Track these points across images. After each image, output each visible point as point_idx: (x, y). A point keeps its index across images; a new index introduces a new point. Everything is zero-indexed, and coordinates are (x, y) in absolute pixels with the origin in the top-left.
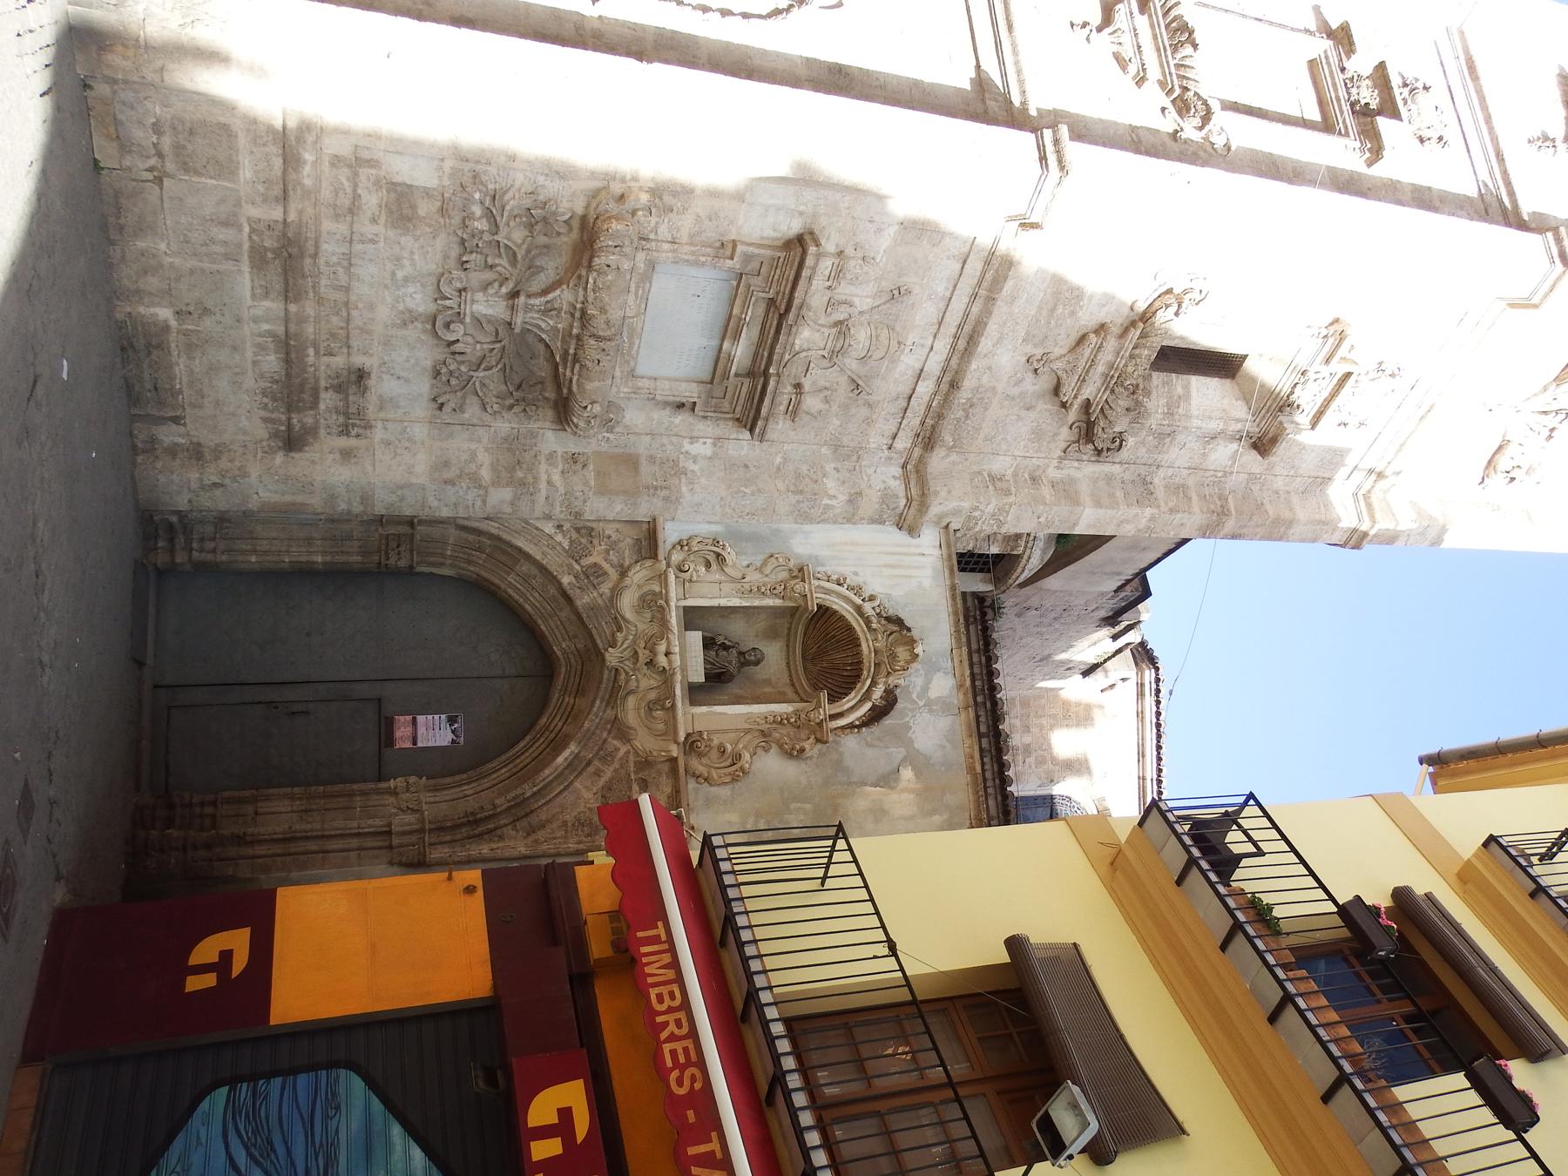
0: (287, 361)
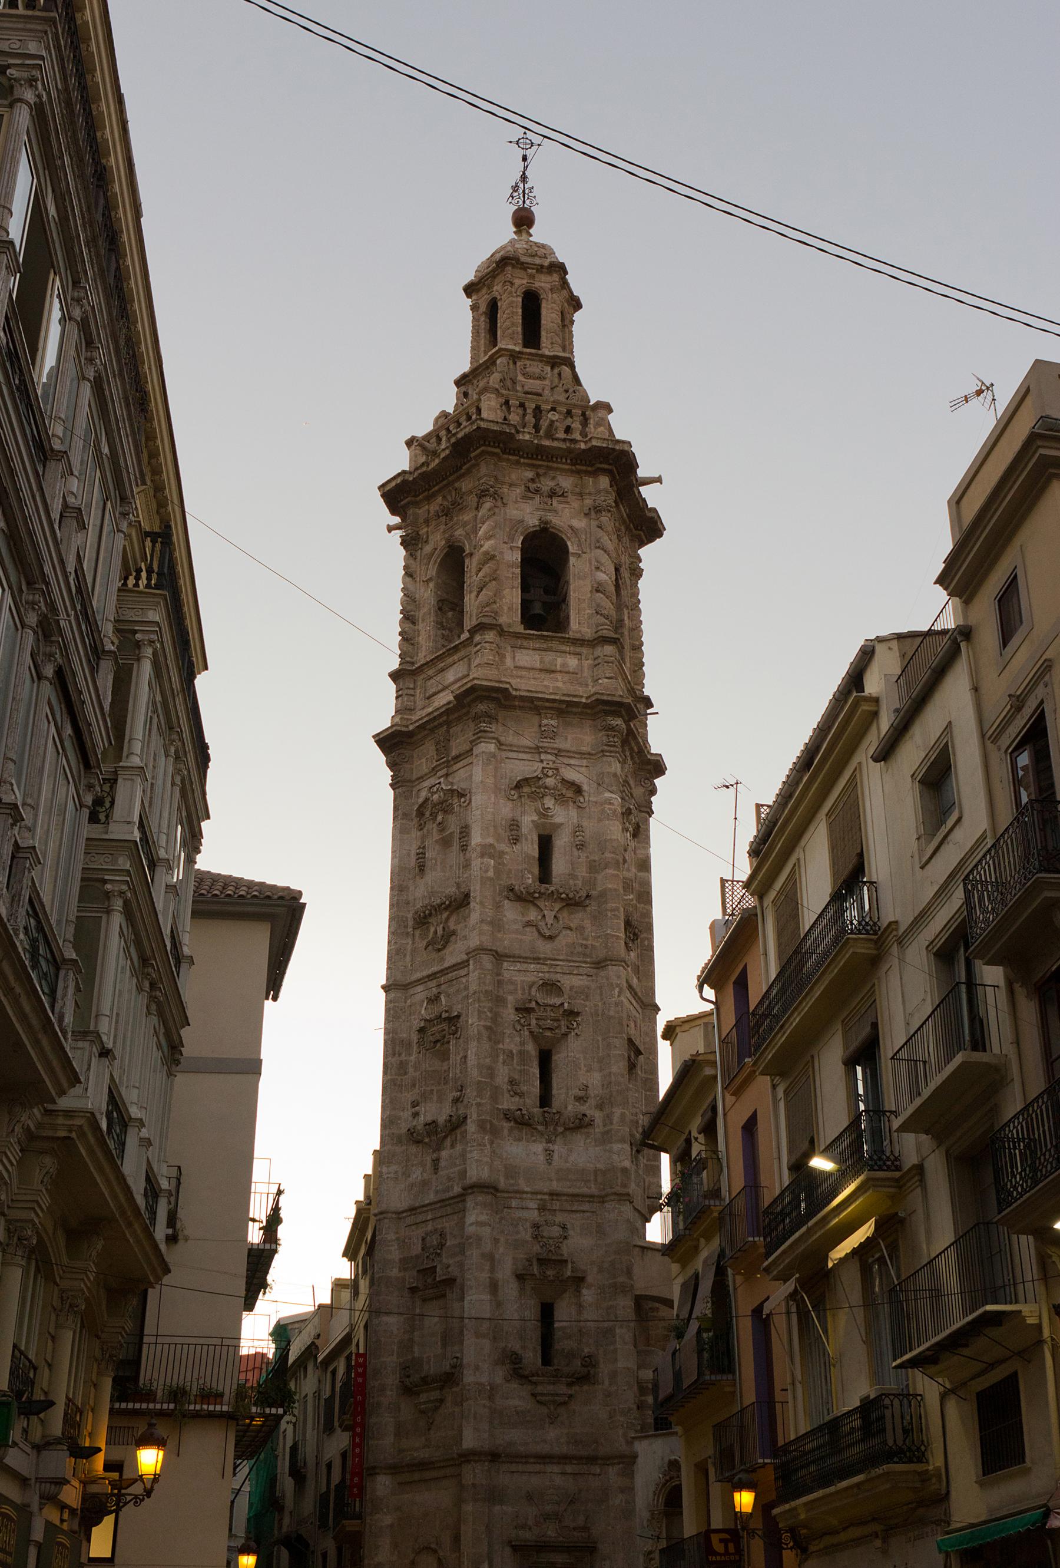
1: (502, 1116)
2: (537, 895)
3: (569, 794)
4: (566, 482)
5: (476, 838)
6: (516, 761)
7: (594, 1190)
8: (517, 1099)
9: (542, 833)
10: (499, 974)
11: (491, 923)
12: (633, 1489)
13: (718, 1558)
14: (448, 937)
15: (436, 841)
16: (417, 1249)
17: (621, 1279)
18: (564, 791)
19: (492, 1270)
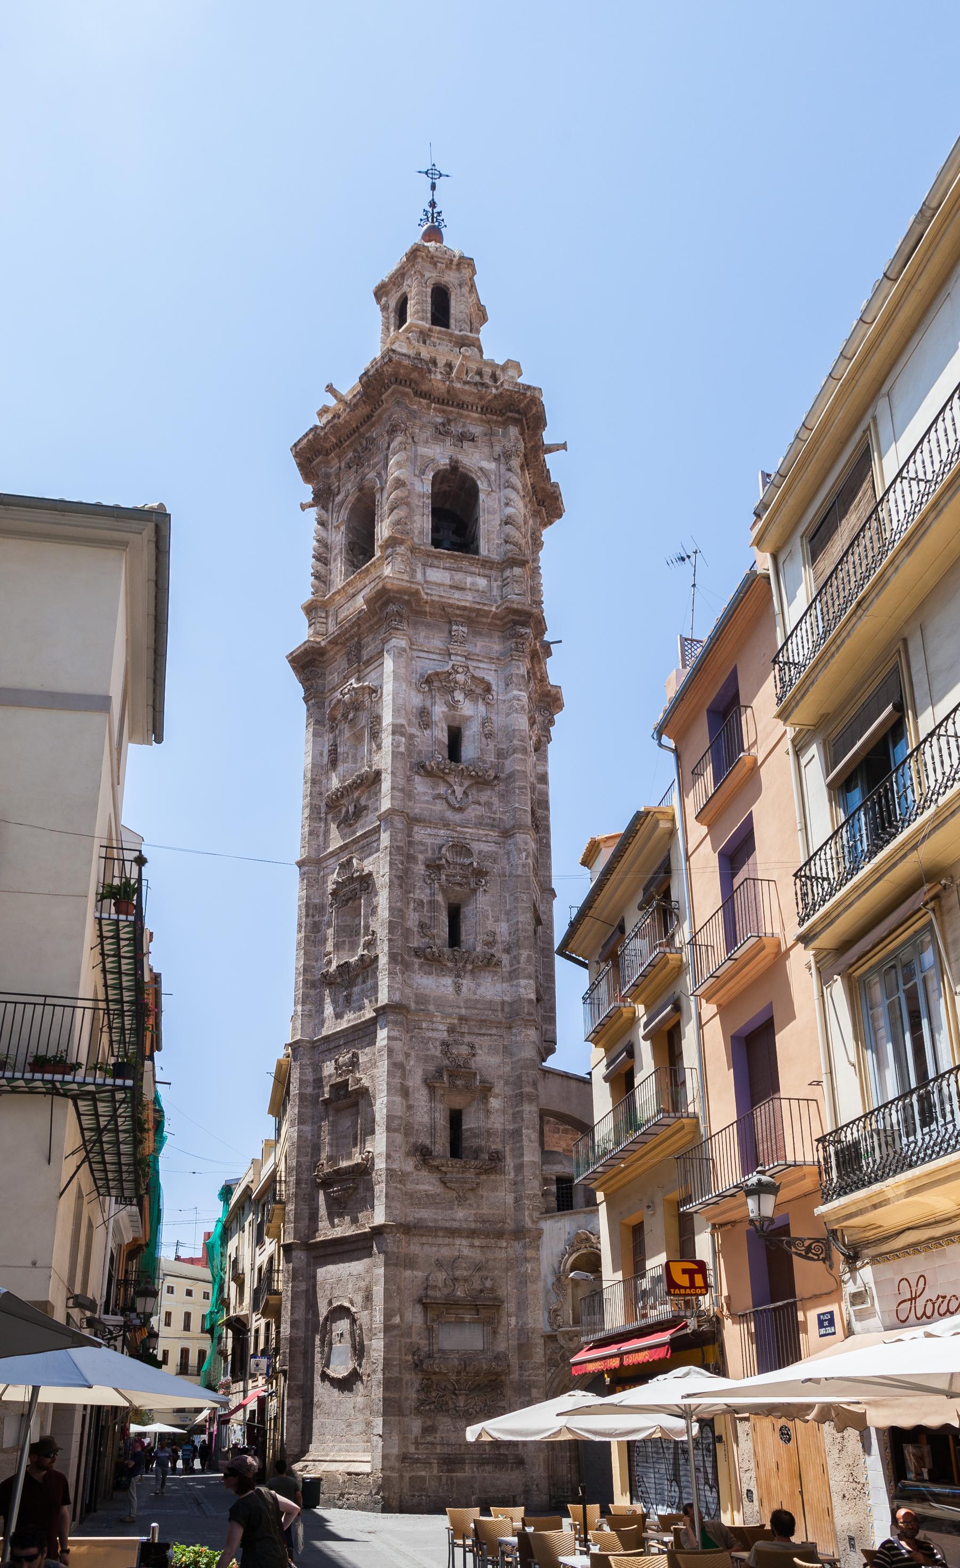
0: (488, 1463)
2: (447, 771)
3: (479, 691)
5: (387, 719)
6: (427, 661)
8: (427, 940)
9: (452, 724)
10: (409, 836)
11: (402, 790)
12: (538, 1259)
14: (359, 812)
15: (348, 738)
17: (527, 1089)
18: (474, 688)
19: (403, 1077)
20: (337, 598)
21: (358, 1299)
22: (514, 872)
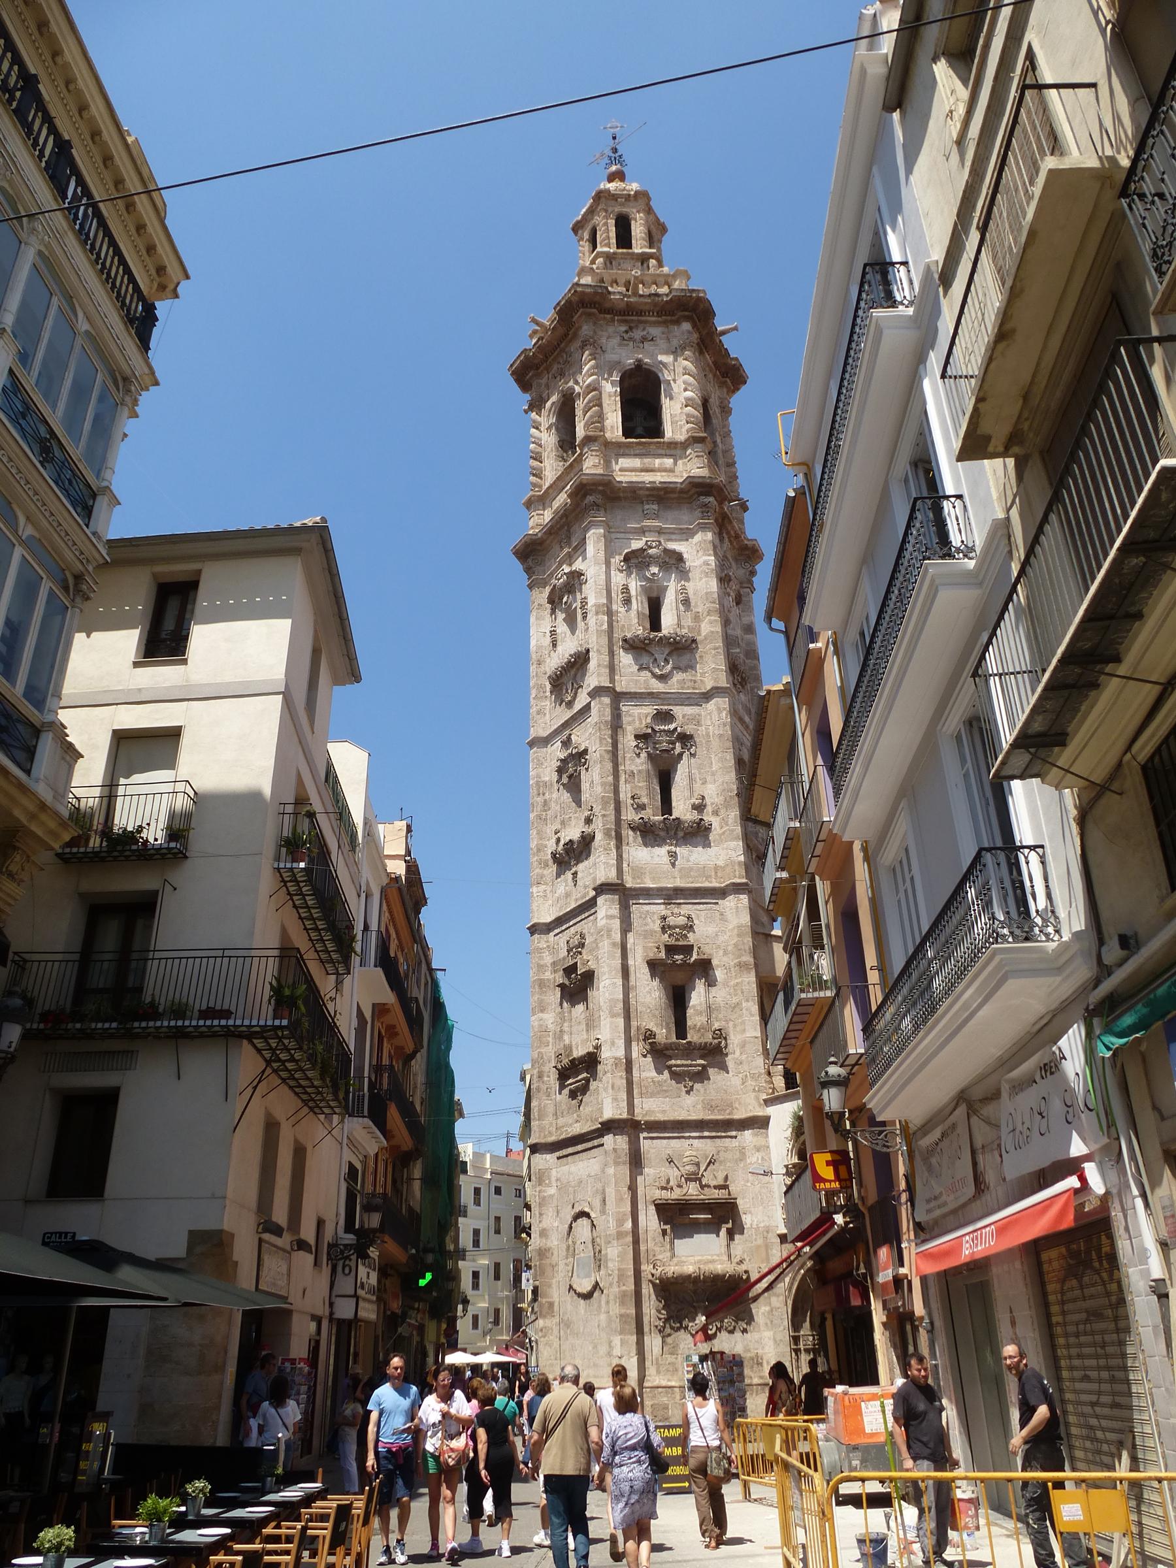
1: (627, 826)
4: (655, 331)
5: (591, 601)
7: (715, 884)
12: (768, 1147)
13: (828, 1185)
16: (563, 953)
20: (551, 491)
21: (597, 1203)
22: (716, 732)
